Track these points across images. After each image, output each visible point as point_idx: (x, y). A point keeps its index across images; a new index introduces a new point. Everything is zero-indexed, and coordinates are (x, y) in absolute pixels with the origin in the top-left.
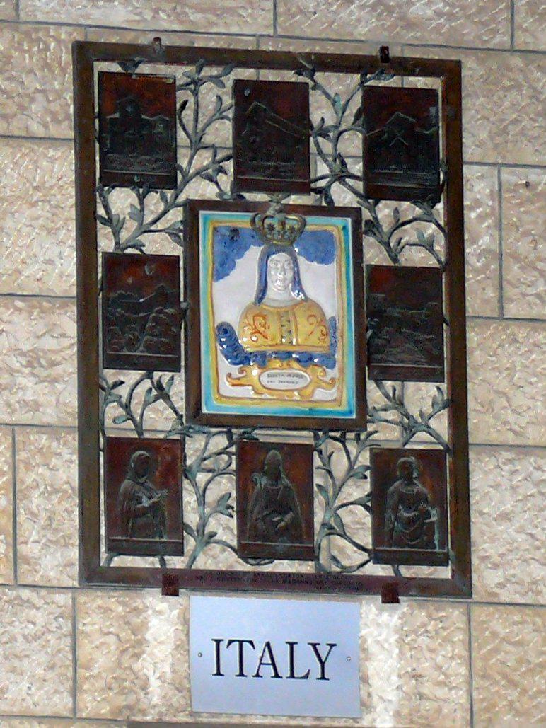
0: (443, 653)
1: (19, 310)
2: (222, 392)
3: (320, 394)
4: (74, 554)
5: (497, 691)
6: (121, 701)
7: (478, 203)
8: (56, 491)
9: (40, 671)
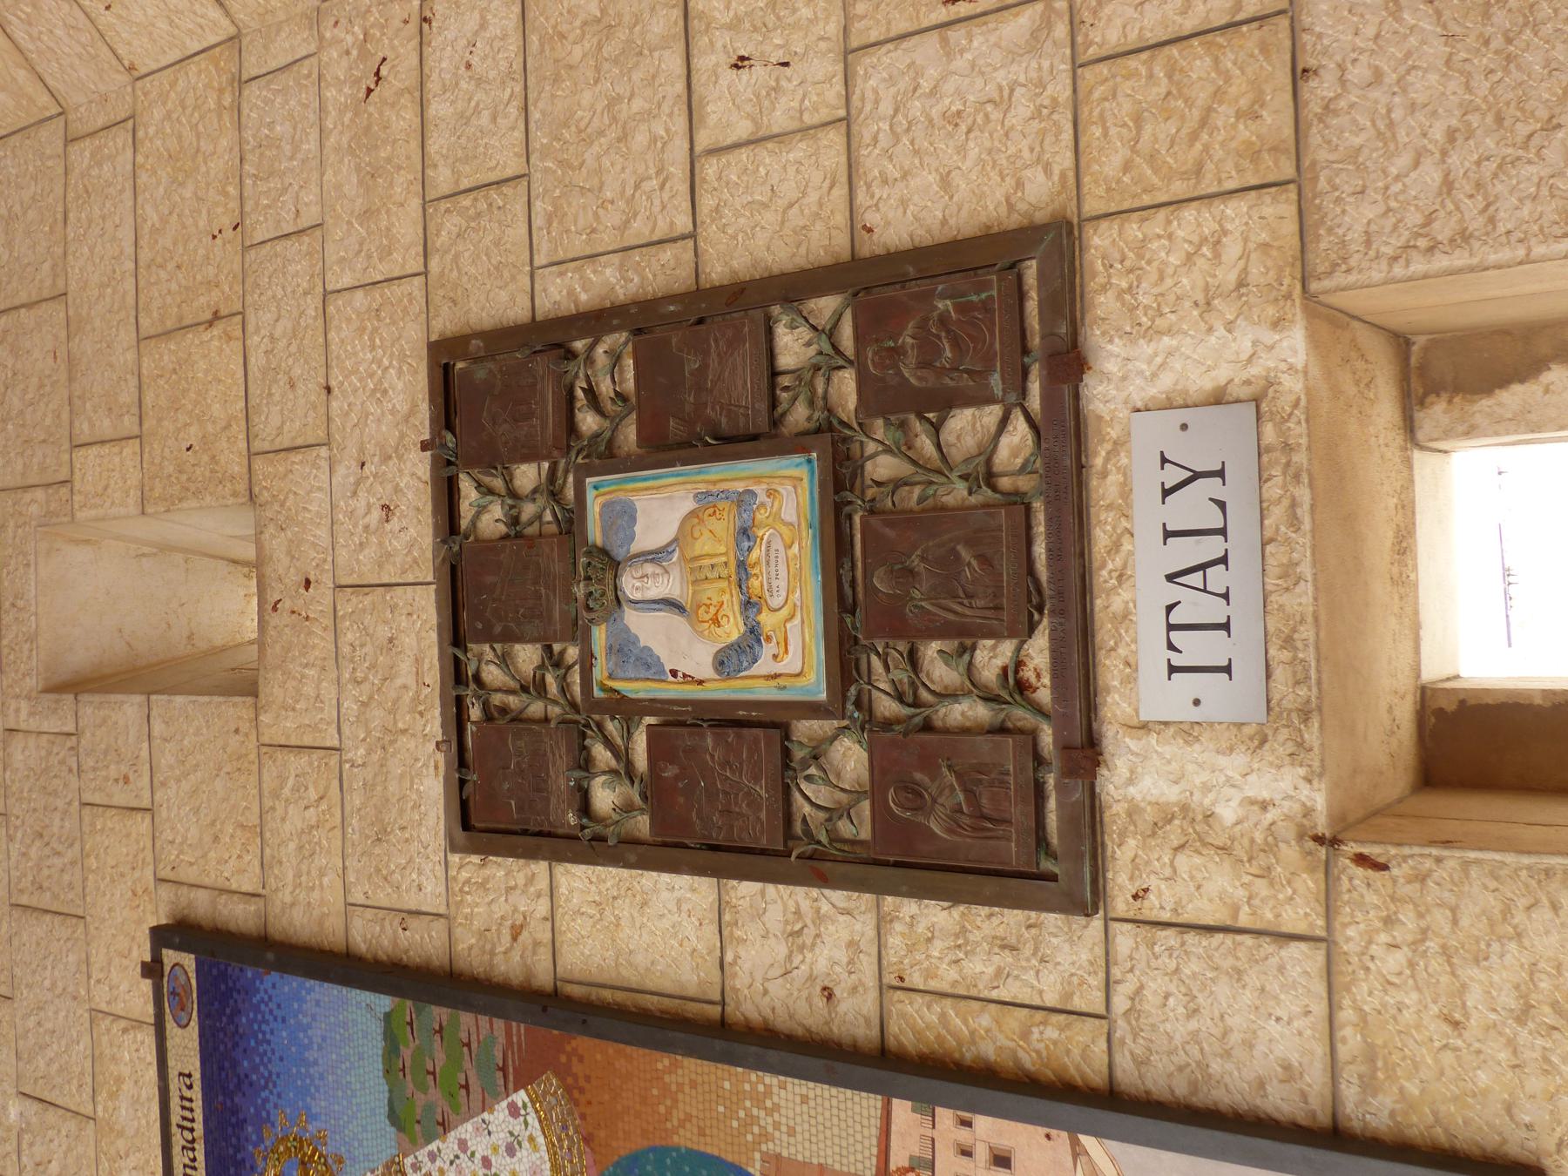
0: (1163, 254)
1: (737, 957)
2: (798, 670)
3: (789, 514)
4: (1052, 919)
5: (1223, 144)
6: (1290, 852)
7: (571, 292)
8: (964, 930)
9: (1248, 997)
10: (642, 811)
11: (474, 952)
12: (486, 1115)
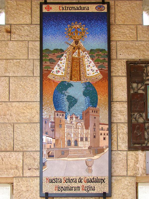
1: (117, 103)
4: (127, 144)
8: (124, 134)
10: (134, 92)
11: (113, 63)
12: (95, 66)
